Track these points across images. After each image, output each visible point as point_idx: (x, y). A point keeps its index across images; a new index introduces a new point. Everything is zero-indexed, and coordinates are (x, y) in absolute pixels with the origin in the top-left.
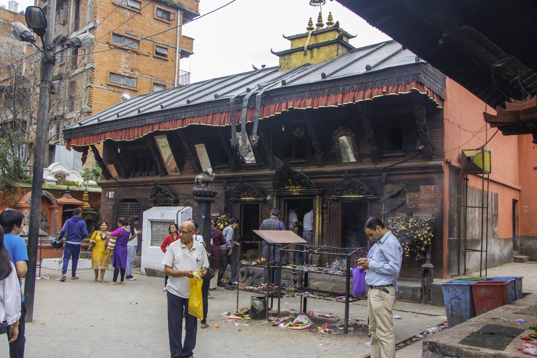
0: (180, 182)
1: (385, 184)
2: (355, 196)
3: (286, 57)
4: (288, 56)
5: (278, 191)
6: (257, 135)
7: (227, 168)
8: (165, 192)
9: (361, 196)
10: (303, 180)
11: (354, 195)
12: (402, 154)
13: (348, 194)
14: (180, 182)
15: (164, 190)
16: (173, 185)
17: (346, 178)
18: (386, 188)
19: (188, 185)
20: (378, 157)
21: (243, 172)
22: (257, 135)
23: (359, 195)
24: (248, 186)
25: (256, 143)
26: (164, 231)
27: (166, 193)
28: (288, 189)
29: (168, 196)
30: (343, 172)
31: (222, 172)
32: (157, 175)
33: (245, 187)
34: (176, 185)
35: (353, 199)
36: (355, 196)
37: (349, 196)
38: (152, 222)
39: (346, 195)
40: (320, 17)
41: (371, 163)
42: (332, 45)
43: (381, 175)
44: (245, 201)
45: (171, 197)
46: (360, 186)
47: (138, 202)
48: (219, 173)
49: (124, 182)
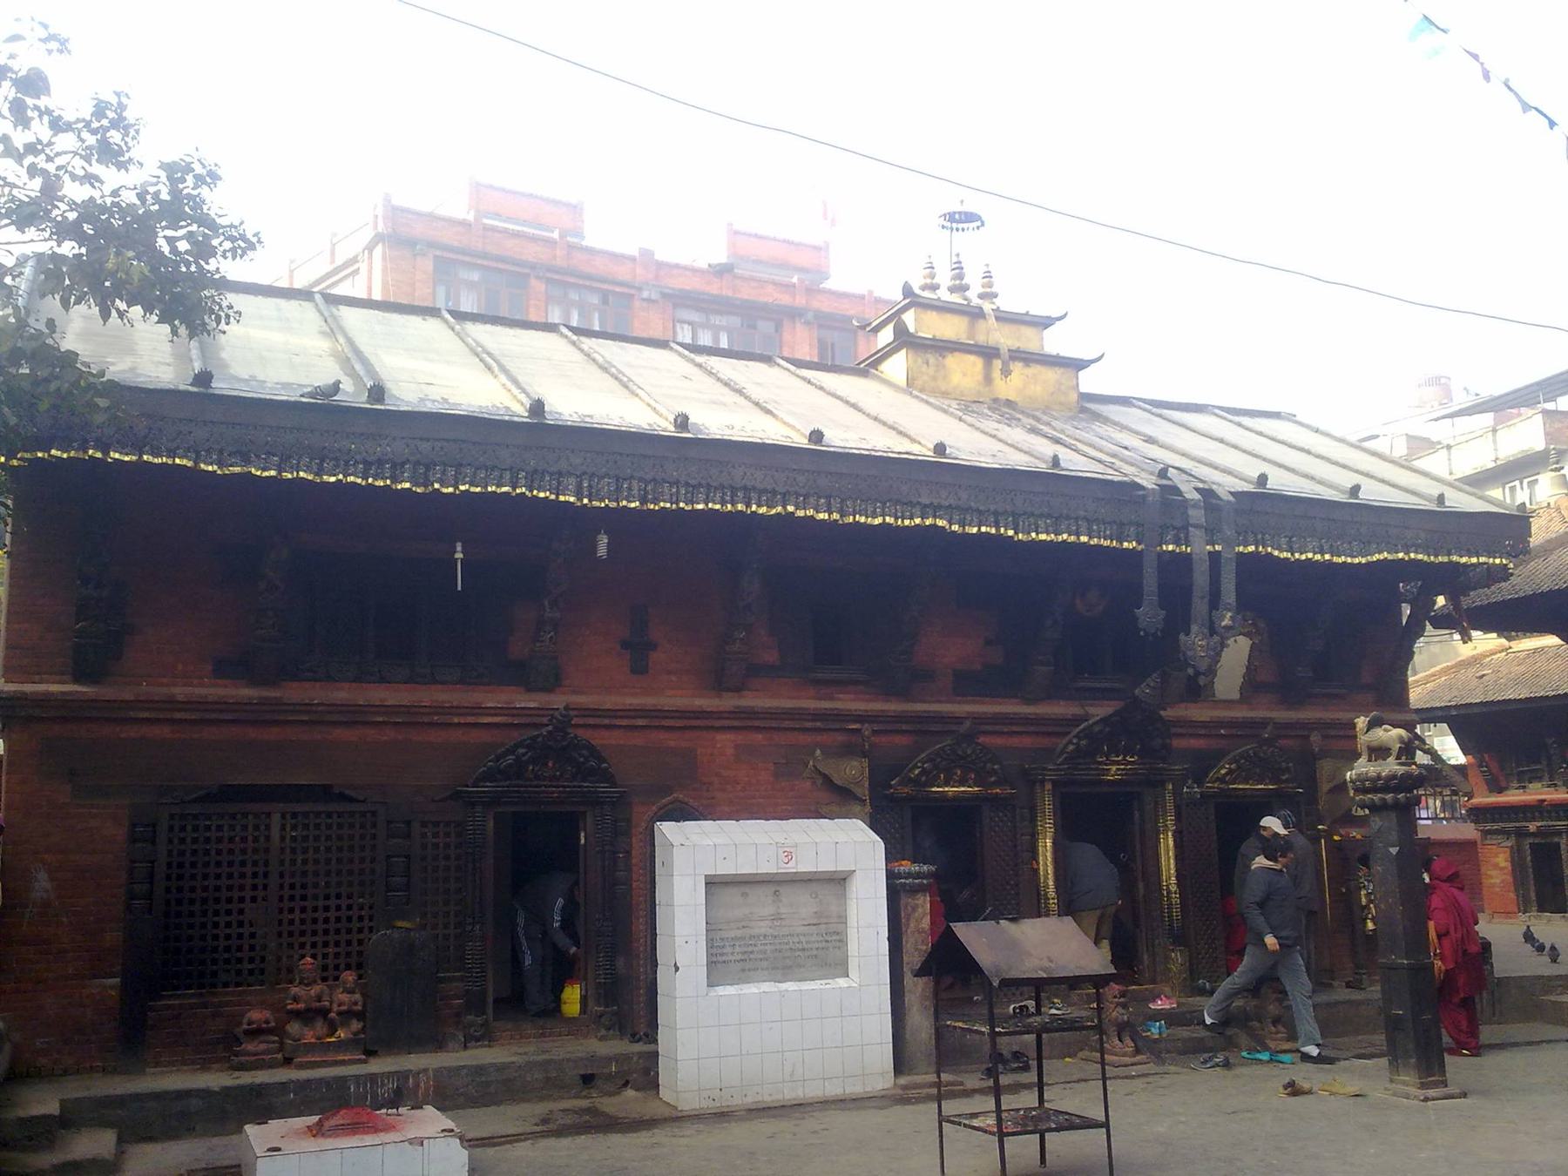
0: (640, 722)
4: (937, 355)
7: (856, 683)
14: (640, 722)
15: (585, 752)
20: (1289, 692)
26: (777, 917)
28: (1100, 763)
30: (1220, 724)
34: (605, 733)
36: (1260, 787)
40: (958, 270)
43: (1309, 736)
47: (351, 800)
48: (832, 699)
49: (263, 702)
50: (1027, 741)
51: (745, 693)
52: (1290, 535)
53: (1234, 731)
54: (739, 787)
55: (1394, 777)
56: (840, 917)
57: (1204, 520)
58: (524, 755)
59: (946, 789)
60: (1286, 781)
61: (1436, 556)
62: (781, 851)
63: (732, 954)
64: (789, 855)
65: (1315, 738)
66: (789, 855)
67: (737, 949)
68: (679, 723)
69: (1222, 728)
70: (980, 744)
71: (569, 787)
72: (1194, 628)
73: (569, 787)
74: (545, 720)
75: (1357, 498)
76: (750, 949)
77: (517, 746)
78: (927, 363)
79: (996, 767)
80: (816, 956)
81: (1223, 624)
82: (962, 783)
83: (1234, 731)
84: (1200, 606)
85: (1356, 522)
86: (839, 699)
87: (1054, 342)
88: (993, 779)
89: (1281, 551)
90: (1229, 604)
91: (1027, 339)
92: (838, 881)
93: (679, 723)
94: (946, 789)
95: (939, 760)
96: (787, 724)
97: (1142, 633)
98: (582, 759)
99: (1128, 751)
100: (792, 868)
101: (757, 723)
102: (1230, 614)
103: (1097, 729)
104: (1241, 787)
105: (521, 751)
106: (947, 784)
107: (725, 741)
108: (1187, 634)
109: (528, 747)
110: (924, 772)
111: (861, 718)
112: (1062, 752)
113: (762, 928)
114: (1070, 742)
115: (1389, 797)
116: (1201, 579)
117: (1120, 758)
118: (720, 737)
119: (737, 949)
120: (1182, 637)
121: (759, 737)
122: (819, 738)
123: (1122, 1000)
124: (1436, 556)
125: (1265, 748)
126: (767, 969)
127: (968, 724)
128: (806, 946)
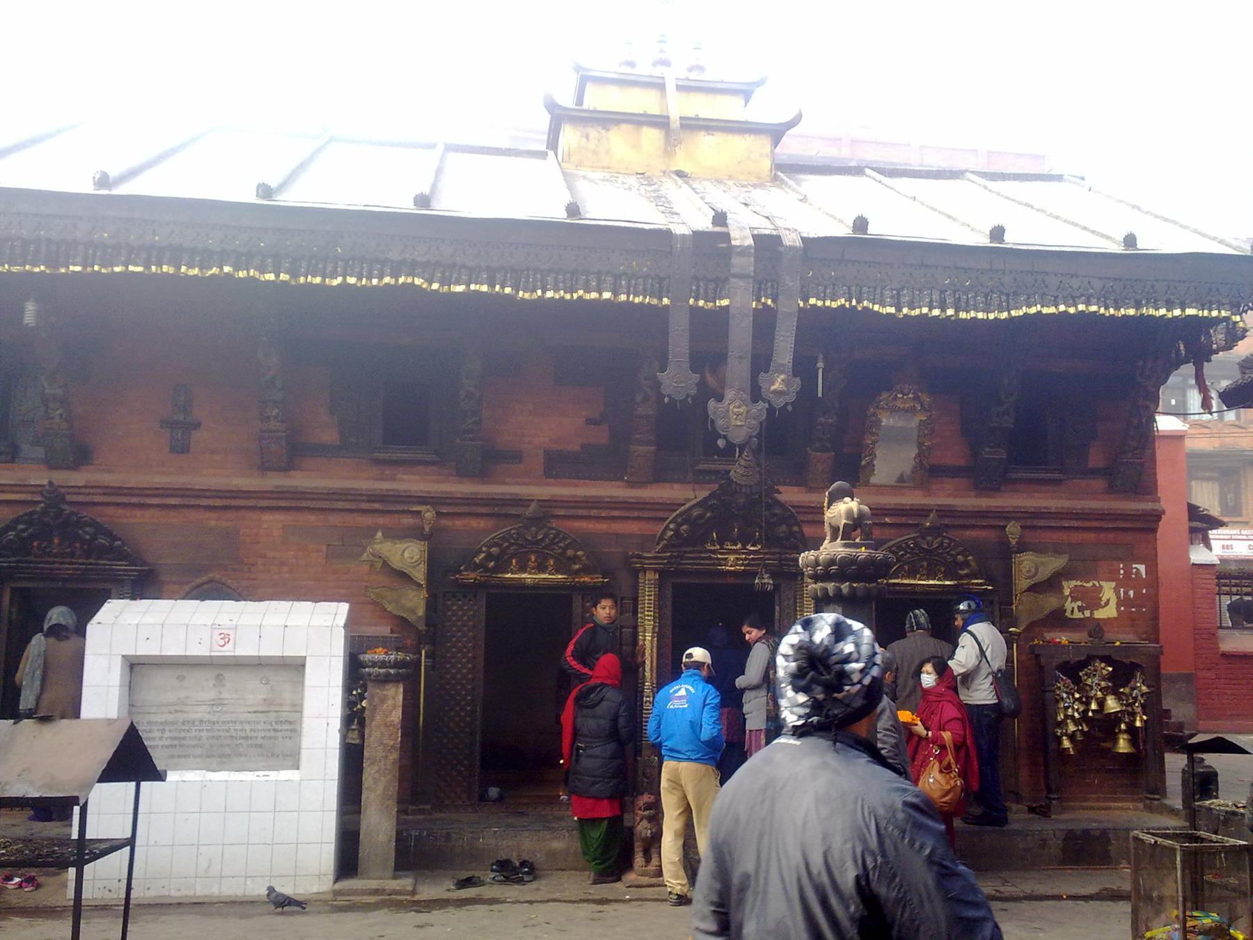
0: (172, 501)
1: (1016, 553)
2: (931, 582)
3: (593, 132)
4: (600, 129)
5: (671, 557)
6: (795, 375)
8: (94, 537)
9: (947, 583)
10: (784, 528)
11: (928, 579)
12: (1057, 476)
13: (912, 574)
14: (172, 501)
16: (120, 511)
17: (935, 531)
18: (1021, 563)
19: (213, 515)
21: (503, 483)
22: (795, 375)
23: (946, 578)
24: (556, 536)
25: (791, 398)
26: (218, 703)
27: (102, 540)
28: (714, 552)
29: (103, 552)
31: (406, 477)
32: (13, 460)
33: (546, 536)
34: (139, 513)
35: (918, 589)
36: (931, 582)
37: (912, 582)
38: (135, 666)
39: (903, 577)
41: (973, 493)
42: (753, 137)
44: (521, 585)
45: (125, 557)
46: (959, 554)
48: (393, 479)
50: (633, 527)
51: (292, 472)
52: (898, 287)
53: (903, 520)
54: (285, 569)
55: (832, 562)
56: (294, 705)
57: (752, 269)
58: (23, 531)
59: (523, 576)
60: (967, 576)
61: (1117, 308)
62: (216, 632)
63: (161, 738)
64: (226, 638)
65: (1013, 529)
66: (226, 638)
67: (167, 734)
68: (218, 503)
69: (886, 515)
70: (553, 528)
71: (83, 564)
72: (729, 394)
73: (83, 564)
74: (38, 498)
75: (1001, 240)
76: (182, 734)
77: (17, 521)
78: (587, 138)
79: (579, 553)
80: (261, 746)
81: (773, 388)
82: (541, 568)
83: (903, 520)
84: (738, 369)
85: (997, 271)
86: (402, 480)
87: (761, 111)
88: (577, 567)
89: (883, 305)
90: (782, 365)
91: (728, 108)
92: (295, 667)
93: (218, 503)
94: (523, 576)
95: (506, 544)
96: (340, 505)
97: (666, 400)
98: (87, 537)
99: (745, 539)
100: (228, 651)
101: (304, 504)
102: (782, 377)
103: (696, 513)
104: (906, 581)
105: (21, 527)
106: (523, 569)
107: (273, 522)
108: (720, 398)
109: (30, 523)
110: (490, 557)
111: (423, 500)
112: (661, 538)
113: (200, 713)
114: (667, 528)
115: (830, 586)
116: (741, 337)
117: (739, 546)
118: (267, 517)
119: (167, 734)
120: (712, 404)
121: (312, 518)
122: (381, 520)
123: (647, 813)
124: (1117, 308)
125: (929, 538)
126: (201, 756)
127: (533, 506)
128: (249, 734)
